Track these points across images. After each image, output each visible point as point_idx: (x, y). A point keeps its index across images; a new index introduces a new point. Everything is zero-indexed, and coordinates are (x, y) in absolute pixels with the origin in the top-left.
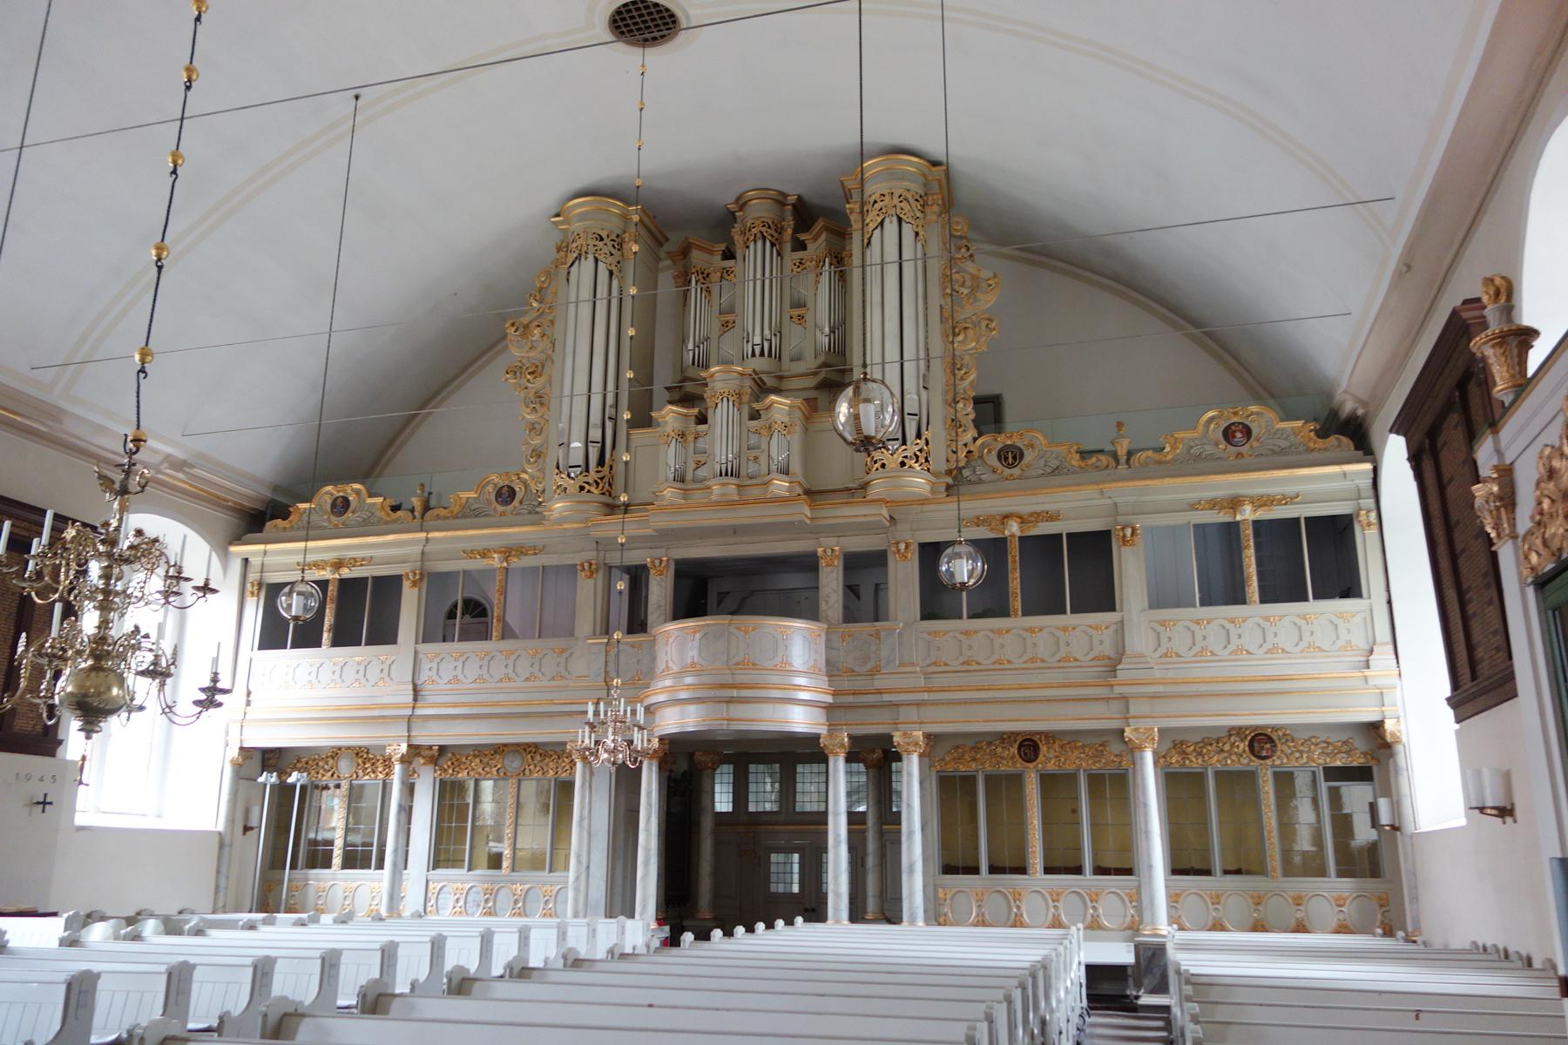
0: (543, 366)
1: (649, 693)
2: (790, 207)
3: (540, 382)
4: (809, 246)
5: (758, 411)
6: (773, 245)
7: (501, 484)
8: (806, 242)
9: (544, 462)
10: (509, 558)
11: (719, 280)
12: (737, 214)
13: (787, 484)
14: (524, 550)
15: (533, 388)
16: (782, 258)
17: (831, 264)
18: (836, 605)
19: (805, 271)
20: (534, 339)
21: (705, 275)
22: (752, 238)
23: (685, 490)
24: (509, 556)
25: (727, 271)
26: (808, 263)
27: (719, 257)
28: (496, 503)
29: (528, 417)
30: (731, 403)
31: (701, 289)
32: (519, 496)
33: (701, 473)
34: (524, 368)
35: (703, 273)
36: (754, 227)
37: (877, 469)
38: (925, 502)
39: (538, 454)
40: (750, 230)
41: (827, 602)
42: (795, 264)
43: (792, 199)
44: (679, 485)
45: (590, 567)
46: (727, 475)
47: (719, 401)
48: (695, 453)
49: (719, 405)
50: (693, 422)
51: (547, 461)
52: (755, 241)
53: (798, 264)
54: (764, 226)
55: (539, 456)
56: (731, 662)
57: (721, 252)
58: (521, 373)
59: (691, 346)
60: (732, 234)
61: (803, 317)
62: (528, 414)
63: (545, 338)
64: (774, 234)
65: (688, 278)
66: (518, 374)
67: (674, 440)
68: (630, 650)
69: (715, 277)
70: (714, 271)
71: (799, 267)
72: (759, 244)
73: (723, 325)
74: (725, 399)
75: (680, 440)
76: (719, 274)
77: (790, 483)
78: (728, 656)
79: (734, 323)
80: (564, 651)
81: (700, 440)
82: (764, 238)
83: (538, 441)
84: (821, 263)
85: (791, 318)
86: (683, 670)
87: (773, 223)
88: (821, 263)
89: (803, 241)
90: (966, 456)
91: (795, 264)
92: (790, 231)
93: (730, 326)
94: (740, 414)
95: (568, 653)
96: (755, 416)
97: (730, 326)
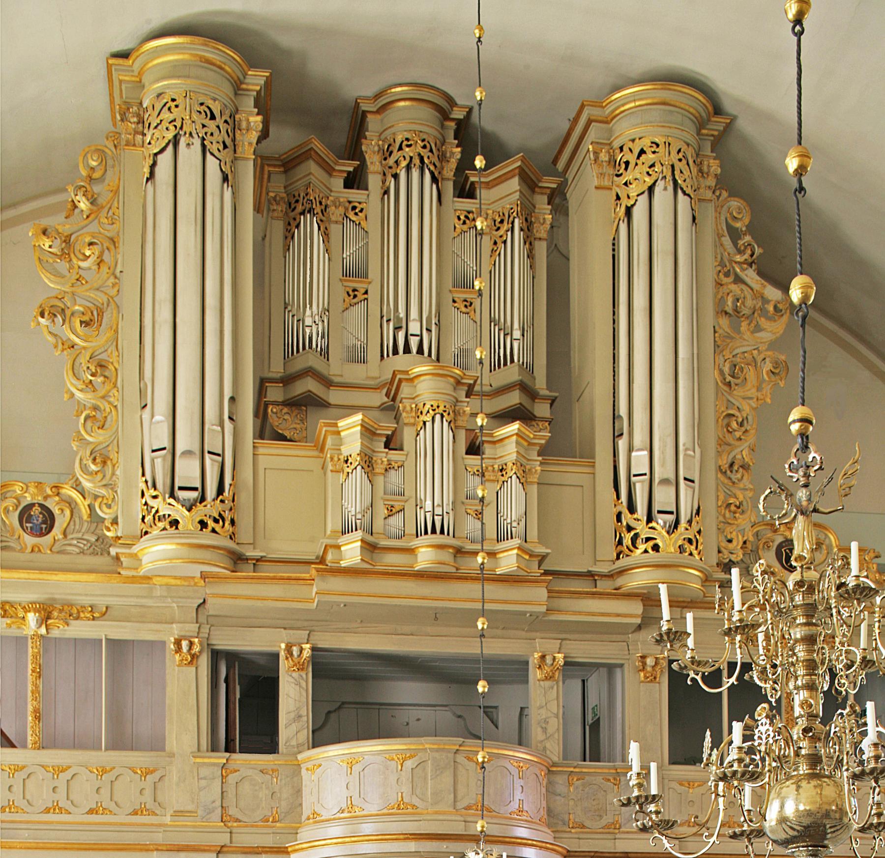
0: (101, 313)
1: (297, 847)
2: (452, 124)
3: (99, 340)
6: (434, 180)
7: (29, 499)
9: (113, 474)
10: (50, 622)
14: (75, 611)
15: (84, 348)
17: (521, 230)
18: (556, 736)
20: (83, 264)
21: (323, 207)
22: (404, 164)
24: (48, 618)
28: (21, 532)
29: (79, 395)
32: (61, 522)
33: (396, 521)
34: (68, 313)
35: (321, 203)
36: (409, 146)
37: (646, 551)
38: (690, 605)
39: (102, 458)
40: (400, 148)
41: (545, 730)
43: (458, 114)
45: (190, 648)
48: (385, 494)
51: (118, 472)
52: (408, 168)
54: (424, 147)
55: (104, 463)
56: (460, 805)
58: (64, 321)
60: (364, 148)
62: (81, 390)
63: (104, 269)
64: (437, 164)
66: (59, 319)
67: (359, 468)
68: (259, 778)
69: (336, 213)
70: (334, 202)
72: (415, 174)
75: (367, 469)
78: (455, 797)
80: (148, 772)
81: (392, 472)
83: (101, 439)
86: (385, 811)
90: (742, 548)
95: (157, 775)
96: (474, 449)
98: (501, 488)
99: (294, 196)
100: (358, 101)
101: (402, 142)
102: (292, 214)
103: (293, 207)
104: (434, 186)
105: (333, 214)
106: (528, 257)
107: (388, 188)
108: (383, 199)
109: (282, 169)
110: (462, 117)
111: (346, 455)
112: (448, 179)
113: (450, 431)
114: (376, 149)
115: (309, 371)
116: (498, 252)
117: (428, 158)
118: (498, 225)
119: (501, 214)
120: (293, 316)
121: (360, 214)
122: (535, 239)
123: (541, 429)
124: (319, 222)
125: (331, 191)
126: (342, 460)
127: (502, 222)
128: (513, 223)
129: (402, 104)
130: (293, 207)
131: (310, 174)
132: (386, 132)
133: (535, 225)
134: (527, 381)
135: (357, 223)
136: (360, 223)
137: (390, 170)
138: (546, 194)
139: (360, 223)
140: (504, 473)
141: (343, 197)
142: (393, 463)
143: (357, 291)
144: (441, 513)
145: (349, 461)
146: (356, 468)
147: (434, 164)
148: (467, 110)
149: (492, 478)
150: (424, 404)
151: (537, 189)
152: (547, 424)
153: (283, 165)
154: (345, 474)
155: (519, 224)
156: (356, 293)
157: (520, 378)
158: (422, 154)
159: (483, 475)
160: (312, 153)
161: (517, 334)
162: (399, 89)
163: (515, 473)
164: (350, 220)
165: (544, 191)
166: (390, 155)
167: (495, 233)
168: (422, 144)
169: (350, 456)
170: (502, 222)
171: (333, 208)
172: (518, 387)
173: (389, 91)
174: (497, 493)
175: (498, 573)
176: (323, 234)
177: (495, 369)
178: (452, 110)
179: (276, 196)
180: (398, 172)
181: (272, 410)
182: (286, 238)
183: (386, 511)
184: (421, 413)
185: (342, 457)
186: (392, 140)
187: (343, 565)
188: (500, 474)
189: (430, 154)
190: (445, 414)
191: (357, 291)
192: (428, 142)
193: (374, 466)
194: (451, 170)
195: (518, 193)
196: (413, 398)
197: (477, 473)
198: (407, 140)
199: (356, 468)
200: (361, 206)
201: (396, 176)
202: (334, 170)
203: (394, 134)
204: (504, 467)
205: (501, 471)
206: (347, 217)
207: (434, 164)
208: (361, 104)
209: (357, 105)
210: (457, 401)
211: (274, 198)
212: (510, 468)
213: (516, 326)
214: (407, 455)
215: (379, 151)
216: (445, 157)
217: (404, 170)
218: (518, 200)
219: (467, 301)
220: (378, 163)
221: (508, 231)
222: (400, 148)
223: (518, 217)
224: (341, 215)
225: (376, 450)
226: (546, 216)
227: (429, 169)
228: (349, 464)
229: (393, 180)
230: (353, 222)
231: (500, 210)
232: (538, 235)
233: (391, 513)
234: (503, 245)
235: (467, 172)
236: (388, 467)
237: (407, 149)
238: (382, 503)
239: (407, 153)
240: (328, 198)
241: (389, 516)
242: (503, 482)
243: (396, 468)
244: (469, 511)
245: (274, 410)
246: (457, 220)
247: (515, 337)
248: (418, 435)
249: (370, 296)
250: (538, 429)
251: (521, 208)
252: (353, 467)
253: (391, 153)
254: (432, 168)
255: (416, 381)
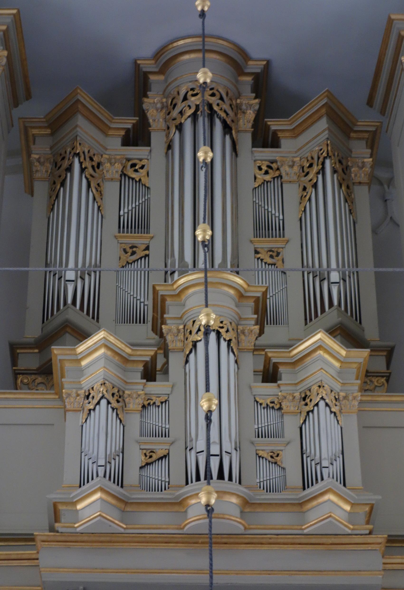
2: (249, 79)
4: (283, 142)
5: (276, 366)
8: (280, 134)
11: (117, 176)
12: (152, 78)
13: (348, 508)
16: (237, 155)
17: (334, 171)
19: (277, 183)
21: (95, 164)
22: (190, 112)
23: (126, 503)
25: (133, 165)
26: (287, 168)
27: (119, 141)
30: (224, 345)
31: (89, 186)
35: (91, 159)
40: (185, 98)
42: (260, 168)
44: (115, 488)
46: (221, 476)
47: (200, 336)
48: (141, 435)
49: (201, 346)
50: (139, 375)
52: (194, 117)
53: (264, 168)
54: (213, 95)
57: (123, 133)
59: (70, 275)
60: (145, 106)
61: (278, 254)
65: (66, 164)
67: (104, 402)
71: (266, 173)
73: (125, 251)
74: (213, 336)
75: (114, 404)
76: (118, 167)
77: (353, 505)
79: (147, 248)
81: (153, 410)
82: (212, 114)
84: (315, 168)
85: (257, 252)
87: (227, 94)
88: (315, 168)
89: (275, 133)
91: (260, 168)
92: (251, 115)
93: (140, 253)
94: (238, 368)
97: (140, 253)
98: (305, 421)
99: (61, 155)
100: (139, 62)
101: (187, 92)
102: (57, 173)
103: (58, 165)
104: (228, 137)
105: (107, 171)
106: (346, 201)
107: (171, 141)
108: (167, 153)
109: (48, 131)
110: (259, 71)
111: (86, 388)
112: (246, 131)
113: (231, 354)
114: (159, 105)
115: (67, 326)
116: (308, 197)
117: (218, 105)
118: (306, 170)
119: (309, 158)
120: (54, 275)
121: (139, 170)
122: (354, 183)
123: (376, 386)
124: (88, 176)
125: (106, 149)
126: (83, 396)
127: (311, 166)
128: (323, 164)
129: (186, 57)
130: (58, 165)
131: (77, 126)
132: (169, 88)
133: (353, 169)
134: (352, 325)
135: (137, 180)
136: (140, 180)
137: (174, 122)
138: (363, 139)
139: (140, 180)
140: (308, 400)
141: (119, 155)
142: (154, 398)
143: (136, 247)
144: (218, 453)
145: (91, 396)
146: (98, 403)
147: (225, 111)
148: (265, 63)
149: (292, 409)
150: (194, 322)
151: (353, 135)
152: (383, 380)
153: (50, 126)
154: (86, 412)
155: (331, 164)
156: (134, 249)
157: (340, 319)
158: (211, 102)
159: (280, 409)
160: (80, 106)
161: (335, 276)
162: (181, 42)
163: (322, 398)
164: (129, 178)
165: (361, 135)
166: (174, 108)
167: (303, 179)
168: (211, 92)
169: (93, 388)
170: (311, 166)
171: (108, 165)
172: (339, 332)
173: (171, 46)
174: (301, 429)
175: (305, 531)
176: (94, 191)
177: (311, 320)
178: (247, 63)
179: (39, 158)
180: (183, 121)
181: (22, 381)
182: (51, 197)
183: (143, 457)
184: (191, 333)
185: (82, 392)
186: (176, 93)
187: (78, 530)
188: (303, 403)
189: (220, 102)
190: (222, 331)
191: (136, 247)
192: (218, 91)
193: (127, 400)
194: (249, 122)
195: (327, 132)
196: (181, 318)
197: (271, 405)
198: (192, 89)
199: (98, 403)
200: (143, 163)
201: (180, 128)
202: (110, 128)
203: (178, 86)
204: (308, 393)
205: (304, 399)
206: (125, 175)
207: (225, 111)
208: (141, 66)
209: (136, 66)
210: (240, 318)
211: (38, 160)
212: (315, 393)
213: (334, 265)
214: (173, 387)
215: (162, 108)
216: (241, 109)
217: (189, 120)
218: (328, 139)
219: (273, 251)
220: (161, 120)
221: (318, 173)
222: (185, 98)
223: (330, 157)
224: (117, 172)
225: (128, 381)
226: (366, 160)
227: (220, 118)
228: (90, 399)
229: (177, 132)
230: (133, 179)
231: (308, 155)
232: (357, 180)
233: (150, 460)
234: (314, 190)
235: (266, 120)
236: (146, 403)
237: (193, 99)
238: (137, 447)
239: (192, 102)
240: (102, 156)
241: (147, 464)
242: (308, 413)
243: (158, 403)
244: (261, 453)
245: (26, 381)
246: (258, 171)
247: (332, 280)
248: (187, 361)
249: (151, 252)
250: (372, 387)
251: (332, 148)
252: (95, 401)
253: (175, 105)
254: (223, 115)
255: (183, 297)
